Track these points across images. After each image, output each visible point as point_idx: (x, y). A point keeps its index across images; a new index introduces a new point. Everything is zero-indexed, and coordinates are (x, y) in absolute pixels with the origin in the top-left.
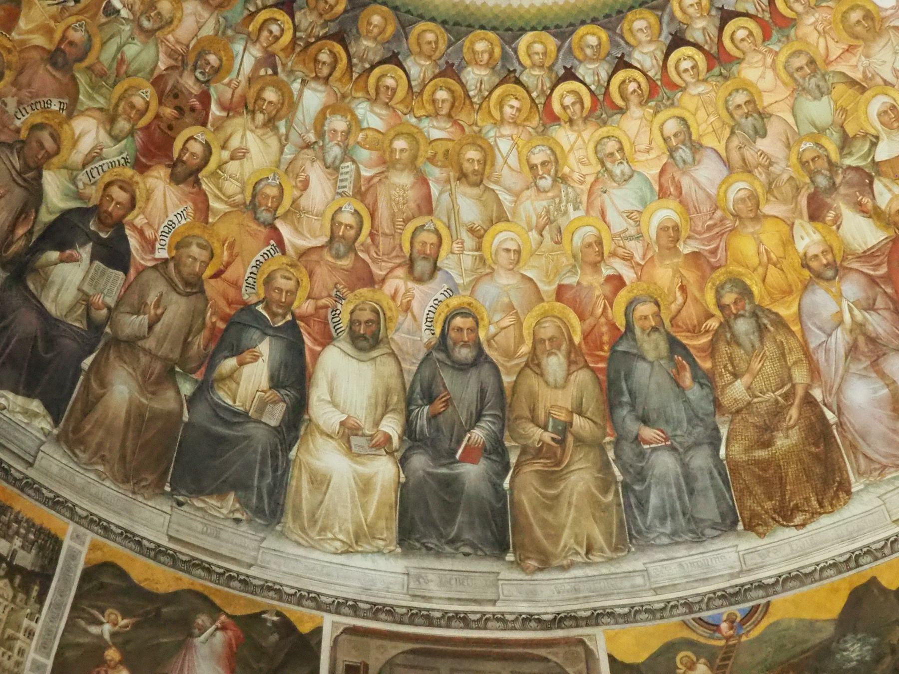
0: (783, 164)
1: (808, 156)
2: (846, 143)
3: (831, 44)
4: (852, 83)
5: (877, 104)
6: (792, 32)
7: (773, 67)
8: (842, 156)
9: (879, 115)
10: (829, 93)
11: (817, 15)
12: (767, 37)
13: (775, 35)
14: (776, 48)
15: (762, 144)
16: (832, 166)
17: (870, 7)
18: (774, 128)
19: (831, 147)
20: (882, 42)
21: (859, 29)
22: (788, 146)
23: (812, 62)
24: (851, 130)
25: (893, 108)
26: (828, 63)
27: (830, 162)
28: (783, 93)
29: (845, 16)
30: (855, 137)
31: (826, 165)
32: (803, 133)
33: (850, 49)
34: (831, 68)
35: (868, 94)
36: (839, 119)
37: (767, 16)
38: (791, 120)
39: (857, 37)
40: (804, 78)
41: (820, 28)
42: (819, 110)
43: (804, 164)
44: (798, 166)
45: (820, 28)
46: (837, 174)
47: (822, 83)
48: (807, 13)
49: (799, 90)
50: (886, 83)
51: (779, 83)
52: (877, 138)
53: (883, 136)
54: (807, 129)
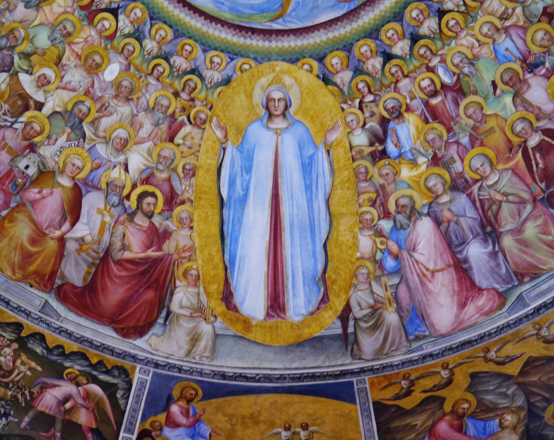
0: (10, 19)
1: (16, 33)
2: (26, 56)
3: (80, 46)
4: (60, 58)
5: (50, 73)
6: (85, 23)
7: (65, 12)
8: (19, 54)
9: (44, 75)
10: (53, 45)
11: (96, 37)
12: (82, 8)
13: (83, 13)
14: (76, 13)
15: (21, 6)
16: (12, 48)
17: (103, 67)
18: (31, 13)
19: (25, 47)
20: (84, 74)
21: (90, 61)
22: (21, 22)
23: (69, 34)
24: (34, 58)
25: (49, 82)
26: (70, 44)
27: (14, 47)
28: (51, 18)
29: (97, 52)
30: (30, 61)
31: (13, 44)
32: (29, 30)
33: (78, 57)
34: (67, 46)
35: (55, 67)
36: (40, 51)
37: (94, 8)
38: (36, 23)
39: (86, 60)
40: (60, 30)
41: (89, 39)
42: (42, 40)
43: (12, 31)
44: (10, 28)
45: (89, 39)
46: (8, 51)
47: (58, 41)
48: (97, 31)
49: (53, 27)
50: (62, 77)
51: (56, 16)
52: (31, 74)
53: (33, 77)
54: (32, 32)
